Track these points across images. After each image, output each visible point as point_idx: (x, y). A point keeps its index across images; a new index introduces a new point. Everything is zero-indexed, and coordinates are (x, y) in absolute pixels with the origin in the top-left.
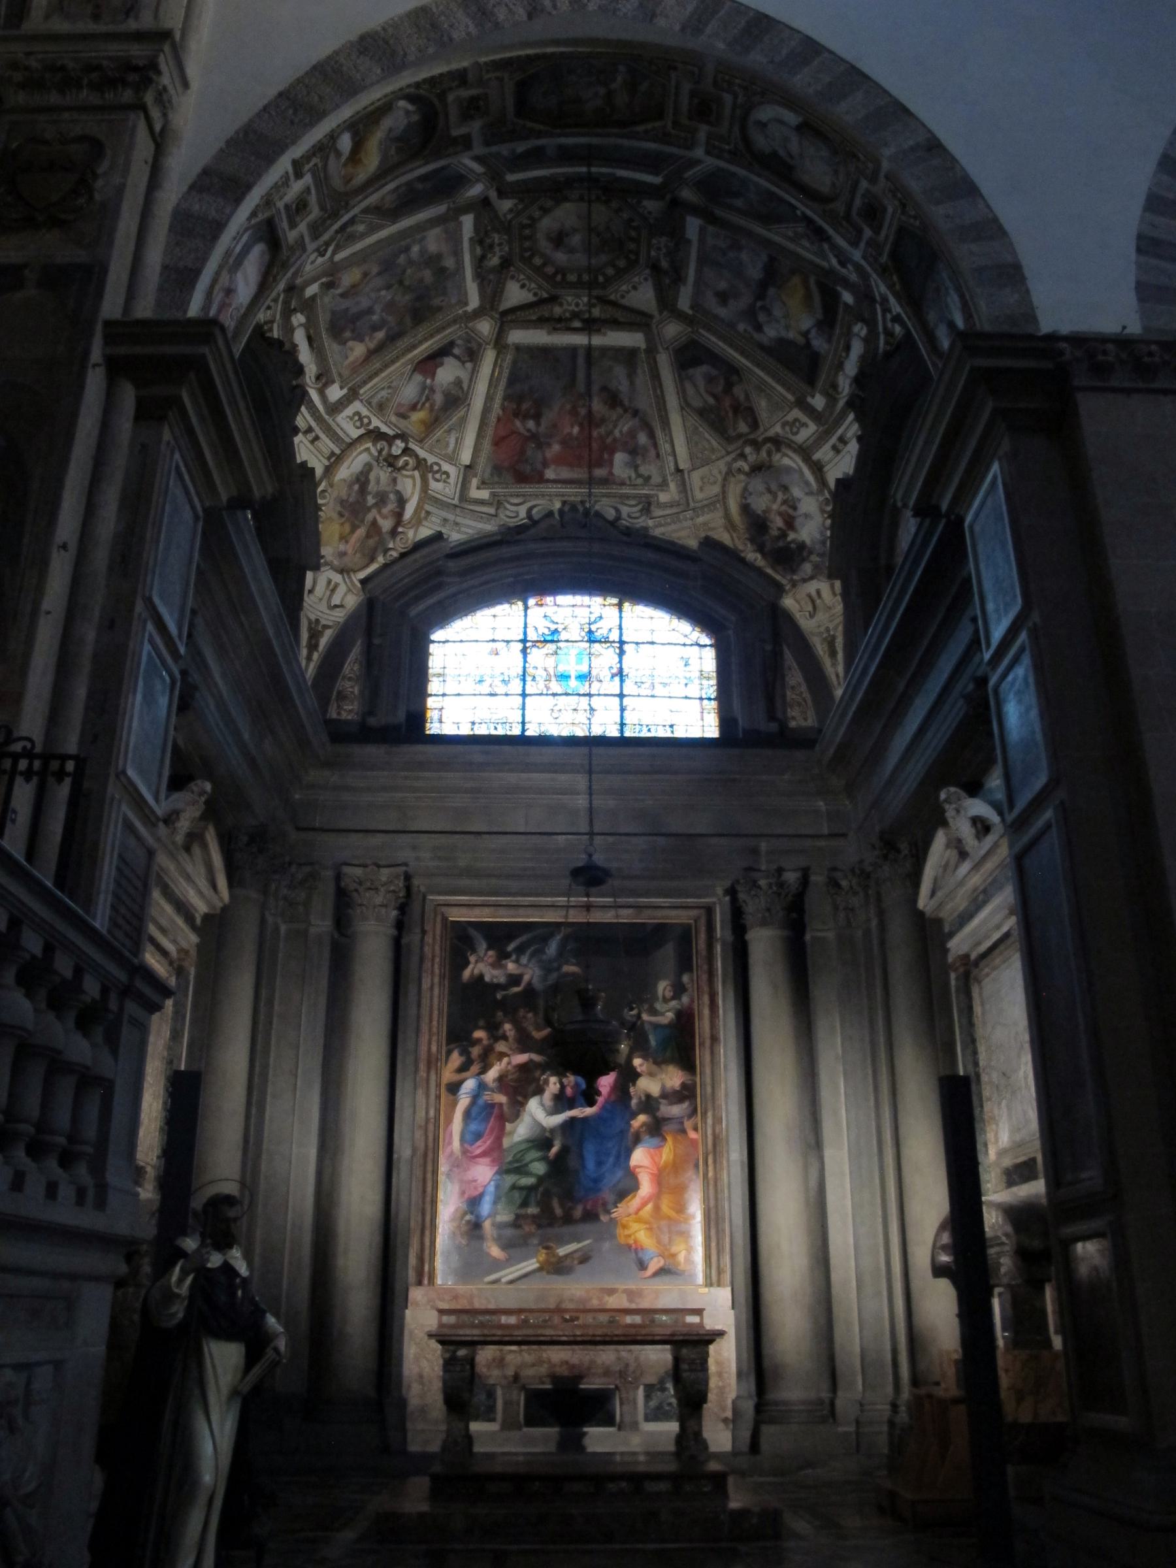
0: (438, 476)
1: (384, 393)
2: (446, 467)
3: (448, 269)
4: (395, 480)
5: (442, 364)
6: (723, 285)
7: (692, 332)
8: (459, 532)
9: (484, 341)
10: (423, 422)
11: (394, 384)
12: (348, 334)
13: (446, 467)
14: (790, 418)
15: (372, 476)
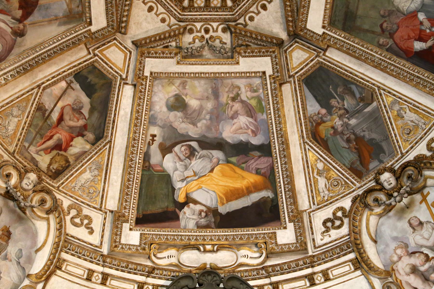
6: (193, 103)
7: (122, 79)
14: (86, 211)
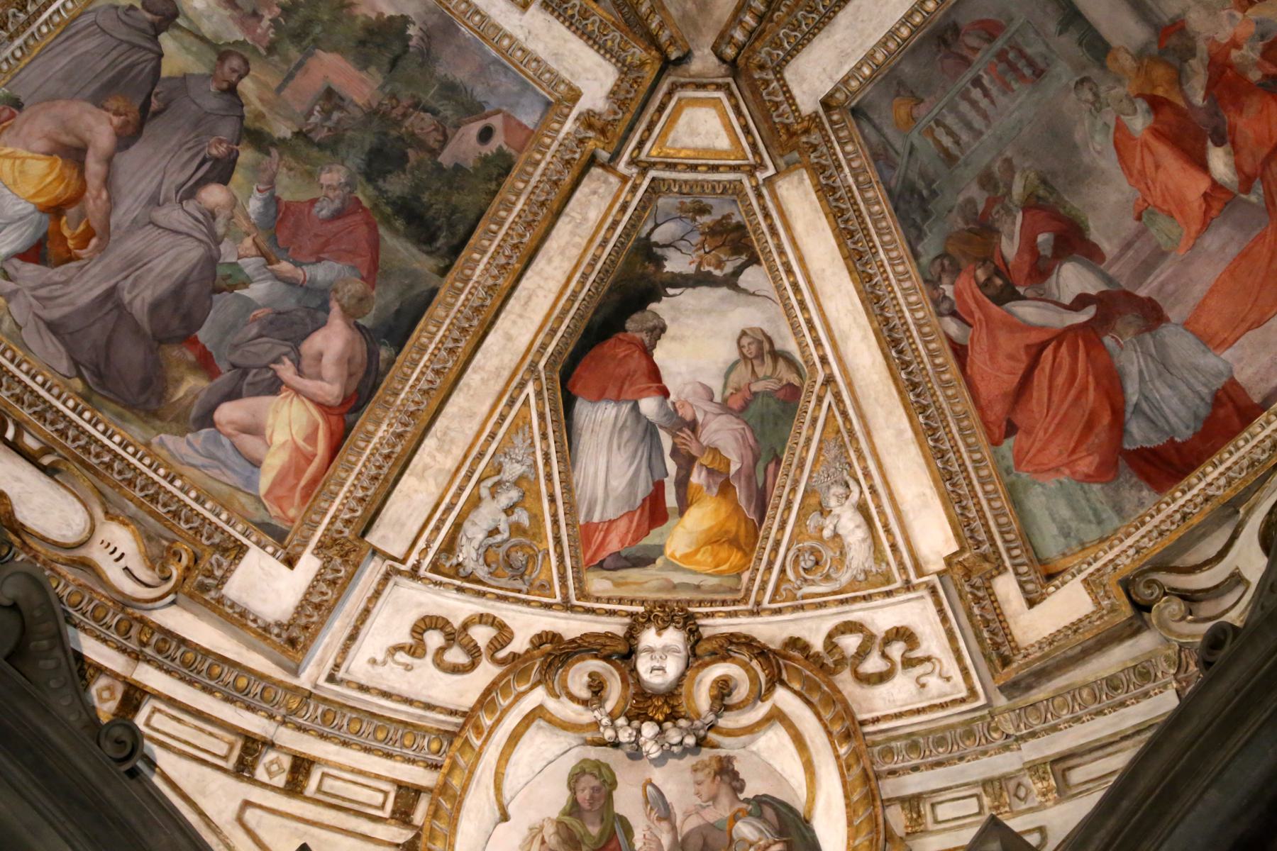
0: (873, 664)
1: (489, 514)
2: (882, 617)
3: (405, 20)
4: (726, 772)
5: (659, 330)
8: (1064, 791)
9: (734, 168)
10: (715, 539)
11: (512, 470)
12: (190, 386)
13: (882, 617)
15: (627, 802)
